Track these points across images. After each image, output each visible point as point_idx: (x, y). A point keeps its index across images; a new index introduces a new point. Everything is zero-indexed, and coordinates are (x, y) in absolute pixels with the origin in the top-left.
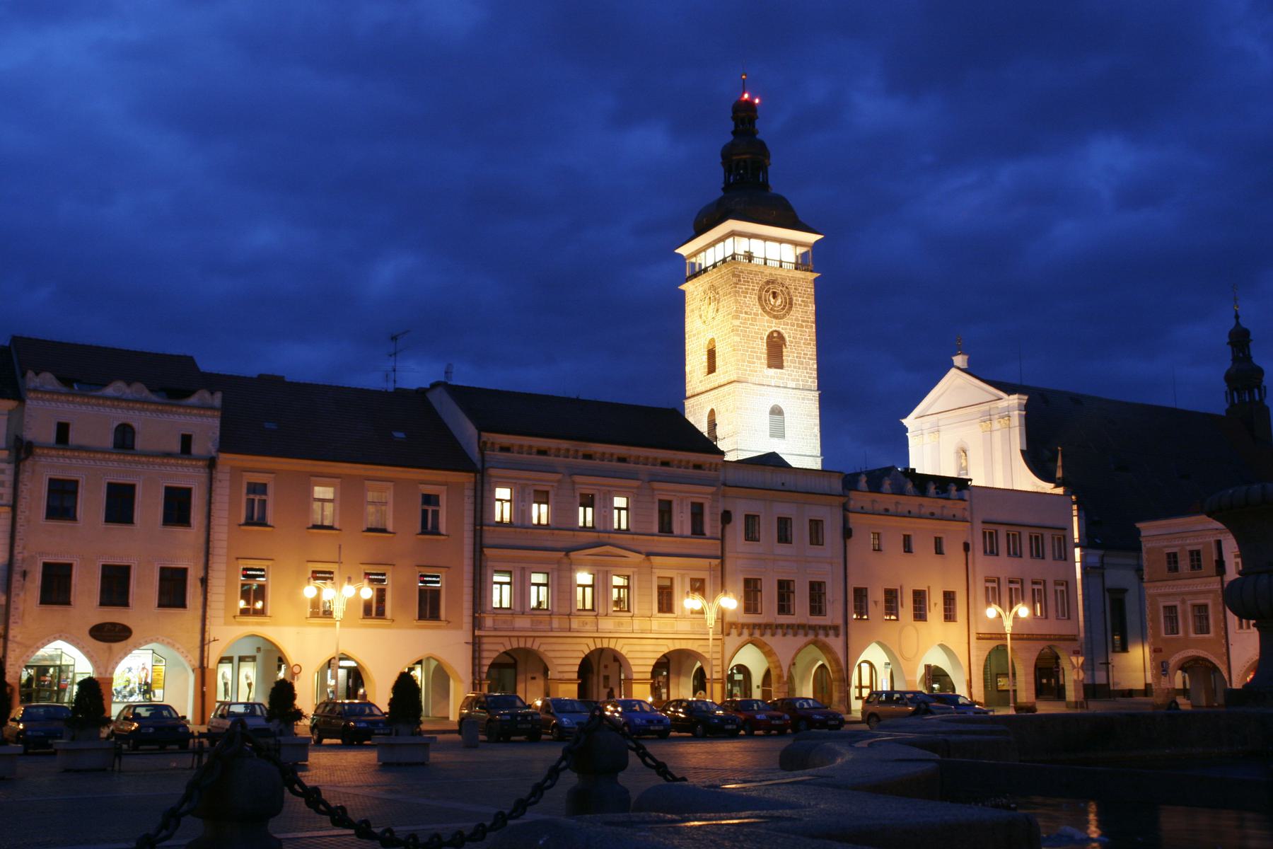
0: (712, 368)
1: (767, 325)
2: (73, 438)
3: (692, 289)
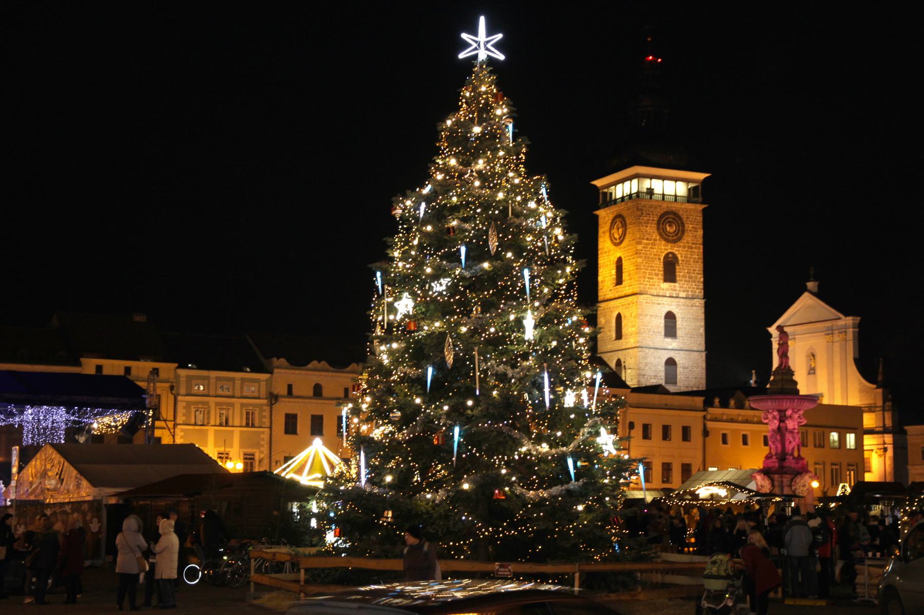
0: (619, 281)
1: (664, 248)
2: (295, 392)
3: (605, 215)
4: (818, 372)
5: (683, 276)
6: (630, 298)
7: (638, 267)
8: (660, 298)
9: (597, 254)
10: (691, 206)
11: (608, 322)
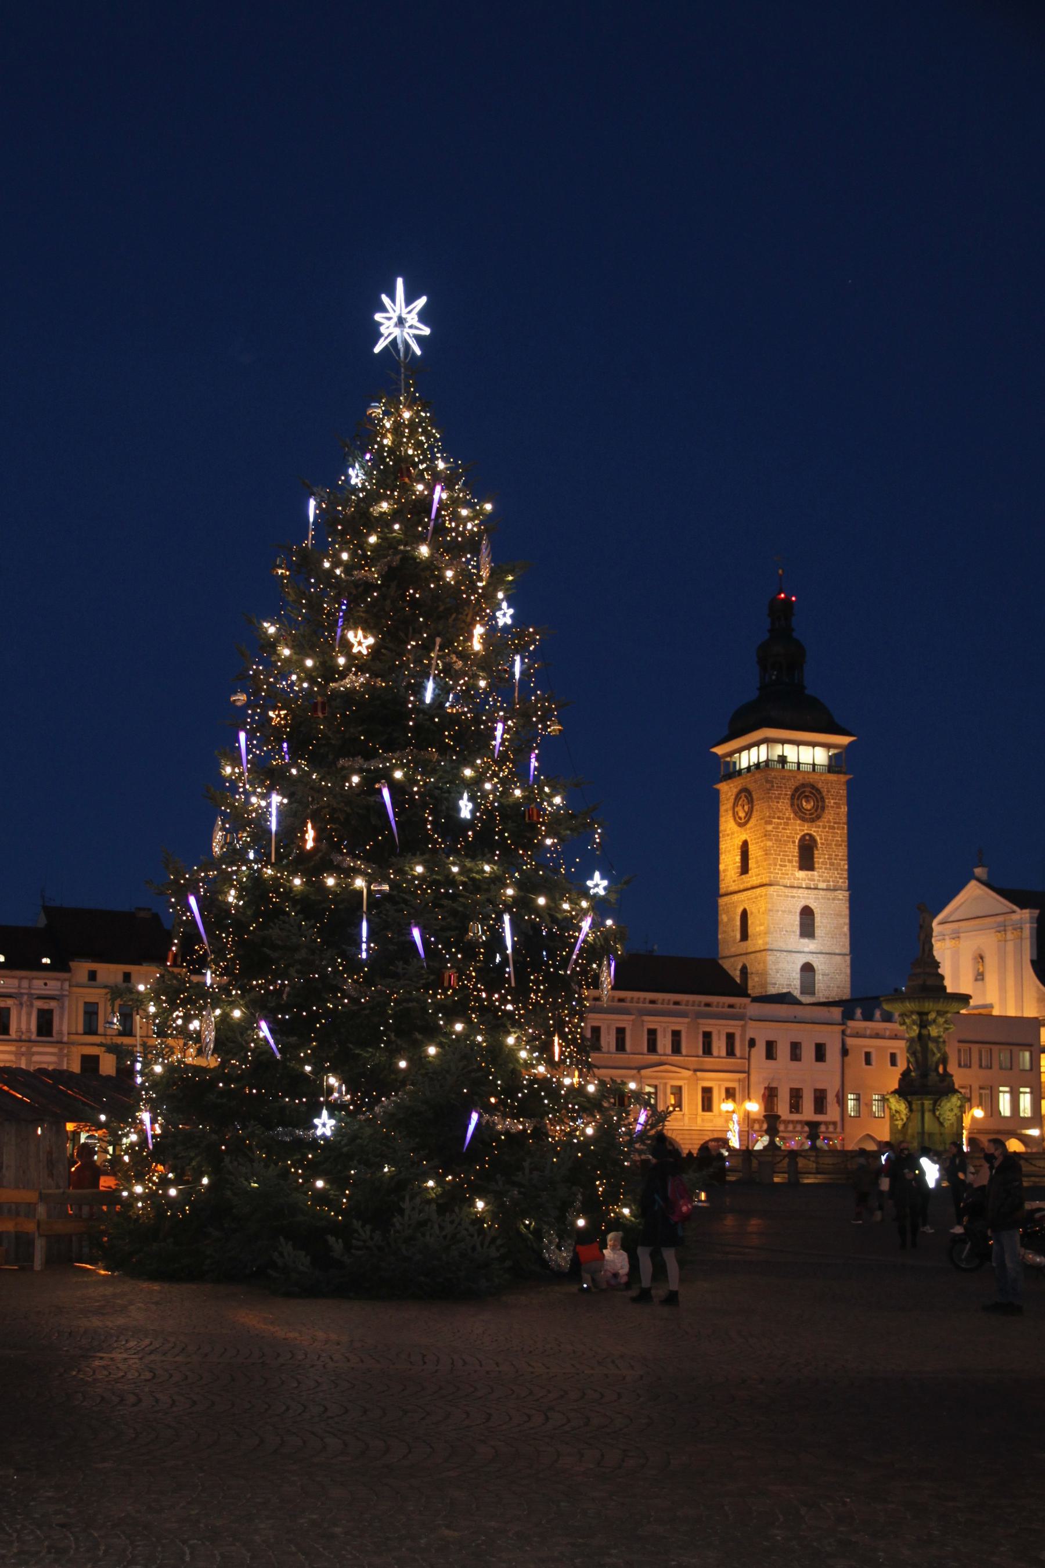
0: (745, 869)
1: (799, 829)
3: (727, 790)
4: (987, 977)
5: (823, 863)
6: (758, 890)
7: (767, 852)
8: (795, 890)
9: (718, 837)
10: (833, 777)
11: (731, 919)
